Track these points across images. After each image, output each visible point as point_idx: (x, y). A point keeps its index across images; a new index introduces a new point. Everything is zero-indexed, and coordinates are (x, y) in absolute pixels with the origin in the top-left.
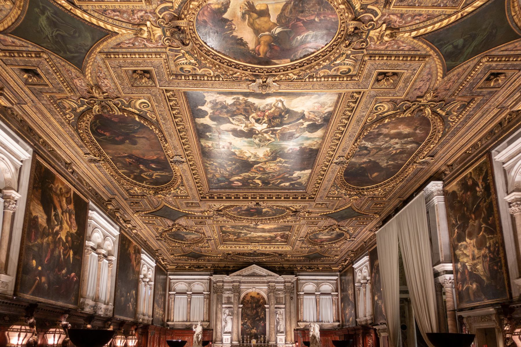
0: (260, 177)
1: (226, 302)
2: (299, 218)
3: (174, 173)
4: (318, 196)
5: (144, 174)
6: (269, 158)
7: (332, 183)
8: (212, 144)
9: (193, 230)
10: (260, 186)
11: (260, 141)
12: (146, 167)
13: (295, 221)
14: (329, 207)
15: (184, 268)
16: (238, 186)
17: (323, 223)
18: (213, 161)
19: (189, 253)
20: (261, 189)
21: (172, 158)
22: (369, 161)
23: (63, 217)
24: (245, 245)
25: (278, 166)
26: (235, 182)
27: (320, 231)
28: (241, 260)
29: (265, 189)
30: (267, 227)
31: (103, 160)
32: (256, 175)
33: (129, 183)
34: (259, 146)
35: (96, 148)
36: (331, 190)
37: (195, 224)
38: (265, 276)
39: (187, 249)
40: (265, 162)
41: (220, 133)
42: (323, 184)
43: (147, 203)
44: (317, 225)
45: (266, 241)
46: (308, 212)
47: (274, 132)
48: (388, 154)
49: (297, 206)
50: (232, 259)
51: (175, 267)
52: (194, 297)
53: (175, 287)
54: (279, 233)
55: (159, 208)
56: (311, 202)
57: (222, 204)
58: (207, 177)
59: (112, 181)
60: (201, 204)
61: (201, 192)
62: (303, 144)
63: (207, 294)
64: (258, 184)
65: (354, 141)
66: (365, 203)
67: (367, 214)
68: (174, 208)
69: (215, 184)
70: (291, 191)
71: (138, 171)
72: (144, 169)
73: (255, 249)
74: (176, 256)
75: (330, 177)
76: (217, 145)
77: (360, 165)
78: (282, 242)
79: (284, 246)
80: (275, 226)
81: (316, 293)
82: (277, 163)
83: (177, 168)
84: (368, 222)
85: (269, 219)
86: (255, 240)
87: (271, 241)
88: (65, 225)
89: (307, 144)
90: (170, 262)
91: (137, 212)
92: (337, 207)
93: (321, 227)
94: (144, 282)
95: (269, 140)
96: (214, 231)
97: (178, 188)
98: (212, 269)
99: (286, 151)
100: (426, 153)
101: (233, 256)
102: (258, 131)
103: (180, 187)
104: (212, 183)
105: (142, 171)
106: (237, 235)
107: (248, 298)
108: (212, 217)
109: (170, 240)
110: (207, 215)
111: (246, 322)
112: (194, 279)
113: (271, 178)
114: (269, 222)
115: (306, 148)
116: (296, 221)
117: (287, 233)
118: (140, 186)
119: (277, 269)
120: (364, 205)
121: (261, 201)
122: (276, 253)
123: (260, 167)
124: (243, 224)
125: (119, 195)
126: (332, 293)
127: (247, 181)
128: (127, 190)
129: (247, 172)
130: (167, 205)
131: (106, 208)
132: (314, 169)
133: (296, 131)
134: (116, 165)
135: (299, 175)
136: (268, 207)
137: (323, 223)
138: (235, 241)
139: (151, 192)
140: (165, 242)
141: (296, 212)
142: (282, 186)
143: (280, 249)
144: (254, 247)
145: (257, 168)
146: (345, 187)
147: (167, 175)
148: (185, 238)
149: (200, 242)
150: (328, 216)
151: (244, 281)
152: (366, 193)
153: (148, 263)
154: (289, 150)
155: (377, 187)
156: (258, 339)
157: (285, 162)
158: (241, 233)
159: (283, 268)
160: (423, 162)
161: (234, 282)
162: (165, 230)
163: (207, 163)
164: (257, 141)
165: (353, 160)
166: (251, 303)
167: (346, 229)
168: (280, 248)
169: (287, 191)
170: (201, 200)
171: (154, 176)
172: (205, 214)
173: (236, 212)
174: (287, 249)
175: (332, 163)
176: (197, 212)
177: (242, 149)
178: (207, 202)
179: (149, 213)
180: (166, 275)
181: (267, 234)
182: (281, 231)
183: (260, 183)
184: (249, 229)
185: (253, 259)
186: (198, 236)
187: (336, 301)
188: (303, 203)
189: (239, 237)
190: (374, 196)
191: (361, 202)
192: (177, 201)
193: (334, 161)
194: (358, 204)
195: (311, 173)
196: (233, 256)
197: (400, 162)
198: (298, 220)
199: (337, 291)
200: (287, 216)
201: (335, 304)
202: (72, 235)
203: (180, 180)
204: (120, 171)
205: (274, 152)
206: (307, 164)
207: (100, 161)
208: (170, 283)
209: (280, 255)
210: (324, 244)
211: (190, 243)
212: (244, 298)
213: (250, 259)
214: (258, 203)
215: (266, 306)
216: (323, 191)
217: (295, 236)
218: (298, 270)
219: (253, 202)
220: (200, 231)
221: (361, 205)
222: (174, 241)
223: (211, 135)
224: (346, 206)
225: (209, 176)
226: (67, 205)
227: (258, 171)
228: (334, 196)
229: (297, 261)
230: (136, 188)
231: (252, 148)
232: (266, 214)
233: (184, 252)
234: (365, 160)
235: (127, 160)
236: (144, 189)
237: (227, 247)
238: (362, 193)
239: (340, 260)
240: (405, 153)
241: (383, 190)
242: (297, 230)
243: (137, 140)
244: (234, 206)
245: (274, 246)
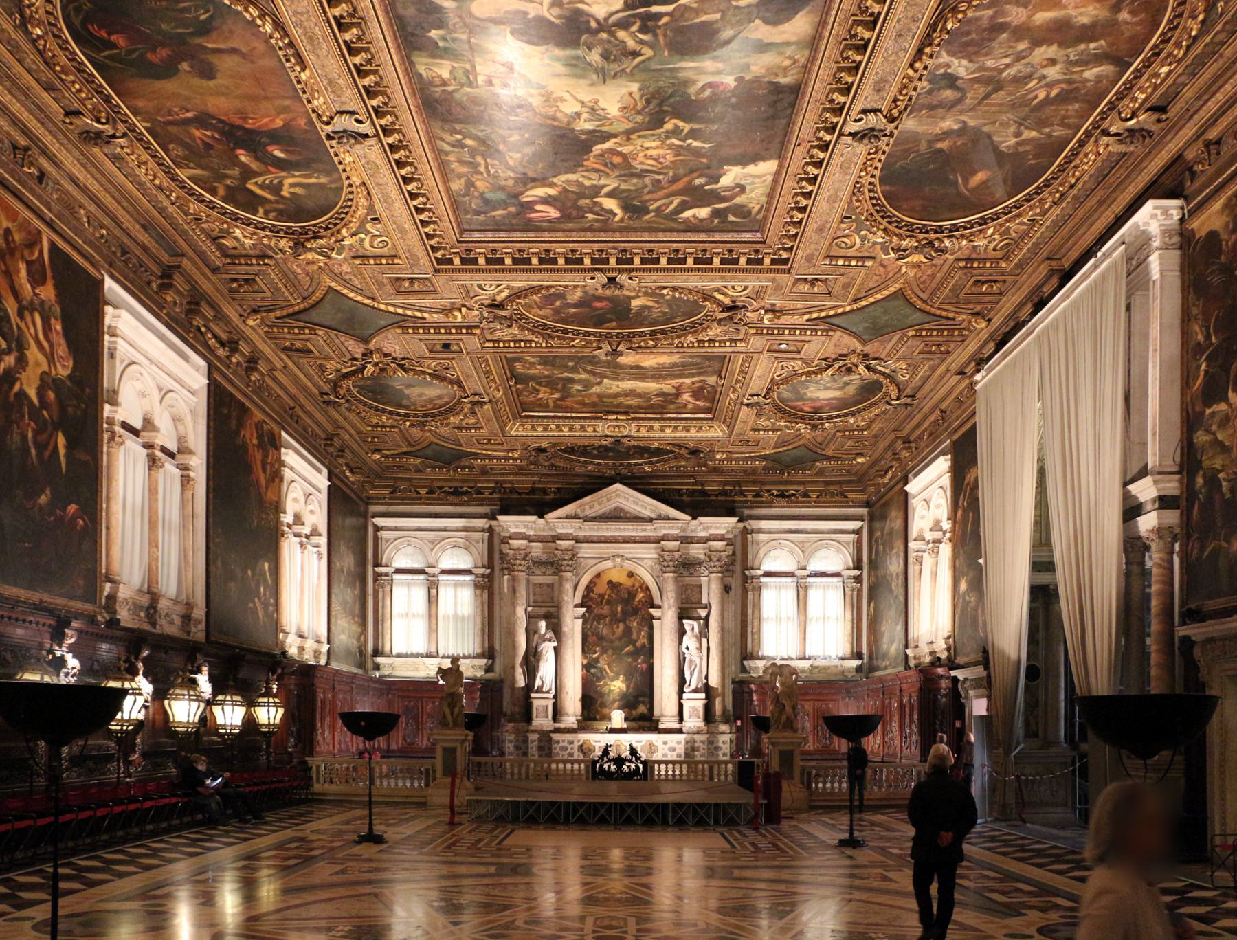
0: (615, 190)
2: (743, 329)
3: (344, 175)
4: (800, 254)
5: (256, 183)
6: (639, 118)
7: (841, 206)
8: (451, 72)
9: (425, 373)
10: (617, 218)
11: (606, 56)
12: (257, 159)
13: (731, 341)
14: (834, 293)
15: (415, 495)
16: (550, 221)
17: (818, 347)
18: (460, 133)
19: (423, 445)
20: (621, 230)
21: (328, 123)
22: (960, 130)
23: (23, 325)
24: (587, 422)
25: (671, 147)
26: (538, 207)
27: (808, 374)
28: (578, 469)
29: (636, 230)
30: (650, 361)
31: (124, 135)
32: (602, 182)
33: (214, 213)
34: (604, 76)
35: (97, 92)
36: (839, 233)
37: (431, 352)
39: (416, 433)
40: (628, 134)
41: (471, 32)
42: (813, 212)
43: (276, 281)
44: (799, 352)
45: (651, 406)
46: (772, 310)
47: (650, 24)
48: (1024, 102)
49: (736, 287)
50: (552, 465)
54: (688, 381)
55: (314, 298)
56: (778, 276)
57: (505, 284)
58: (448, 190)
59: (165, 209)
60: (440, 281)
61: (433, 242)
62: (747, 67)
64: (611, 212)
65: (911, 51)
66: (944, 279)
67: (951, 315)
68: (359, 298)
69: (478, 213)
70: (717, 237)
71: (236, 172)
72: (254, 166)
73: (617, 433)
74: (387, 457)
75: (837, 185)
76: (467, 73)
77: (930, 143)
78: (697, 410)
79: (705, 425)
80: (675, 358)
82: (667, 138)
83: (348, 159)
84: (952, 345)
85: (653, 333)
86: (618, 406)
87: (662, 407)
88: (33, 353)
89: (760, 65)
91: (255, 311)
92: (858, 290)
93: (812, 360)
94: (297, 535)
95: (635, 54)
96: (488, 374)
97: (361, 228)
98: (496, 496)
99: (692, 91)
100: (1143, 96)
101: (553, 456)
102: (598, 21)
103: (368, 226)
104: (467, 212)
105: (248, 174)
106: (560, 386)
108: (477, 327)
109: (365, 404)
110: (459, 319)
113: (650, 192)
114: (651, 343)
115: (756, 80)
116: (736, 341)
117: (712, 380)
118: (249, 225)
119: (685, 498)
120: (941, 283)
121: (624, 270)
122: (680, 446)
123: (612, 151)
124: (573, 350)
125: (191, 253)
127: (576, 201)
128: (215, 239)
129: (572, 170)
130: (339, 288)
131: (161, 300)
132: (785, 158)
133: (722, 18)
134: (166, 150)
135: (738, 181)
136: (646, 294)
137: (818, 347)
138: (557, 408)
139: (284, 244)
140: (349, 410)
141: (733, 308)
142: (687, 221)
143: (693, 433)
144: (615, 427)
145: (602, 155)
146: (884, 222)
147: (322, 186)
148: (408, 397)
149: (451, 410)
150: (829, 324)
152: (947, 243)
153: (305, 480)
154: (703, 89)
155: (983, 221)
157: (693, 134)
158: (572, 381)
159: (704, 493)
160: (1131, 131)
162: (345, 371)
163: (443, 140)
164: (595, 57)
165: (909, 124)
167: (886, 367)
168: (693, 430)
169: (702, 237)
170: (436, 271)
171: (286, 187)
172: (455, 317)
173: (547, 312)
174: (711, 434)
175: (841, 134)
176: (429, 312)
177: (550, 88)
178: (455, 276)
179: (288, 316)
181: (651, 386)
182: (693, 375)
183: (618, 211)
184: (596, 369)
185: (615, 467)
186: (445, 392)
188: (754, 276)
189: (566, 393)
190: (974, 256)
191: (933, 276)
192: (367, 272)
193: (847, 130)
194: (924, 282)
195: (777, 174)
196: (553, 456)
197: (1058, 132)
198: (740, 337)
200: (706, 324)
202: (57, 384)
203: (363, 202)
204: (182, 174)
205: (653, 97)
206: (762, 141)
207: (114, 136)
209: (695, 452)
211: (425, 416)
213: (607, 466)
214: (615, 279)
216: (815, 237)
217: (735, 390)
218: (747, 502)
219: (598, 275)
220: (447, 373)
221: (934, 285)
222: (376, 409)
223: (444, 39)
224: (886, 288)
225: (456, 186)
226: (33, 288)
227: (606, 165)
228: (850, 253)
229: (745, 472)
230: (237, 231)
231: (582, 82)
232: (640, 318)
233: (410, 444)
234: (949, 124)
235: (197, 133)
236: (262, 233)
237: (533, 426)
238: (936, 243)
239: (872, 471)
240: (1076, 100)
241: (1001, 235)
242: (741, 371)
243: (214, 59)
244: (540, 288)
245: (673, 424)
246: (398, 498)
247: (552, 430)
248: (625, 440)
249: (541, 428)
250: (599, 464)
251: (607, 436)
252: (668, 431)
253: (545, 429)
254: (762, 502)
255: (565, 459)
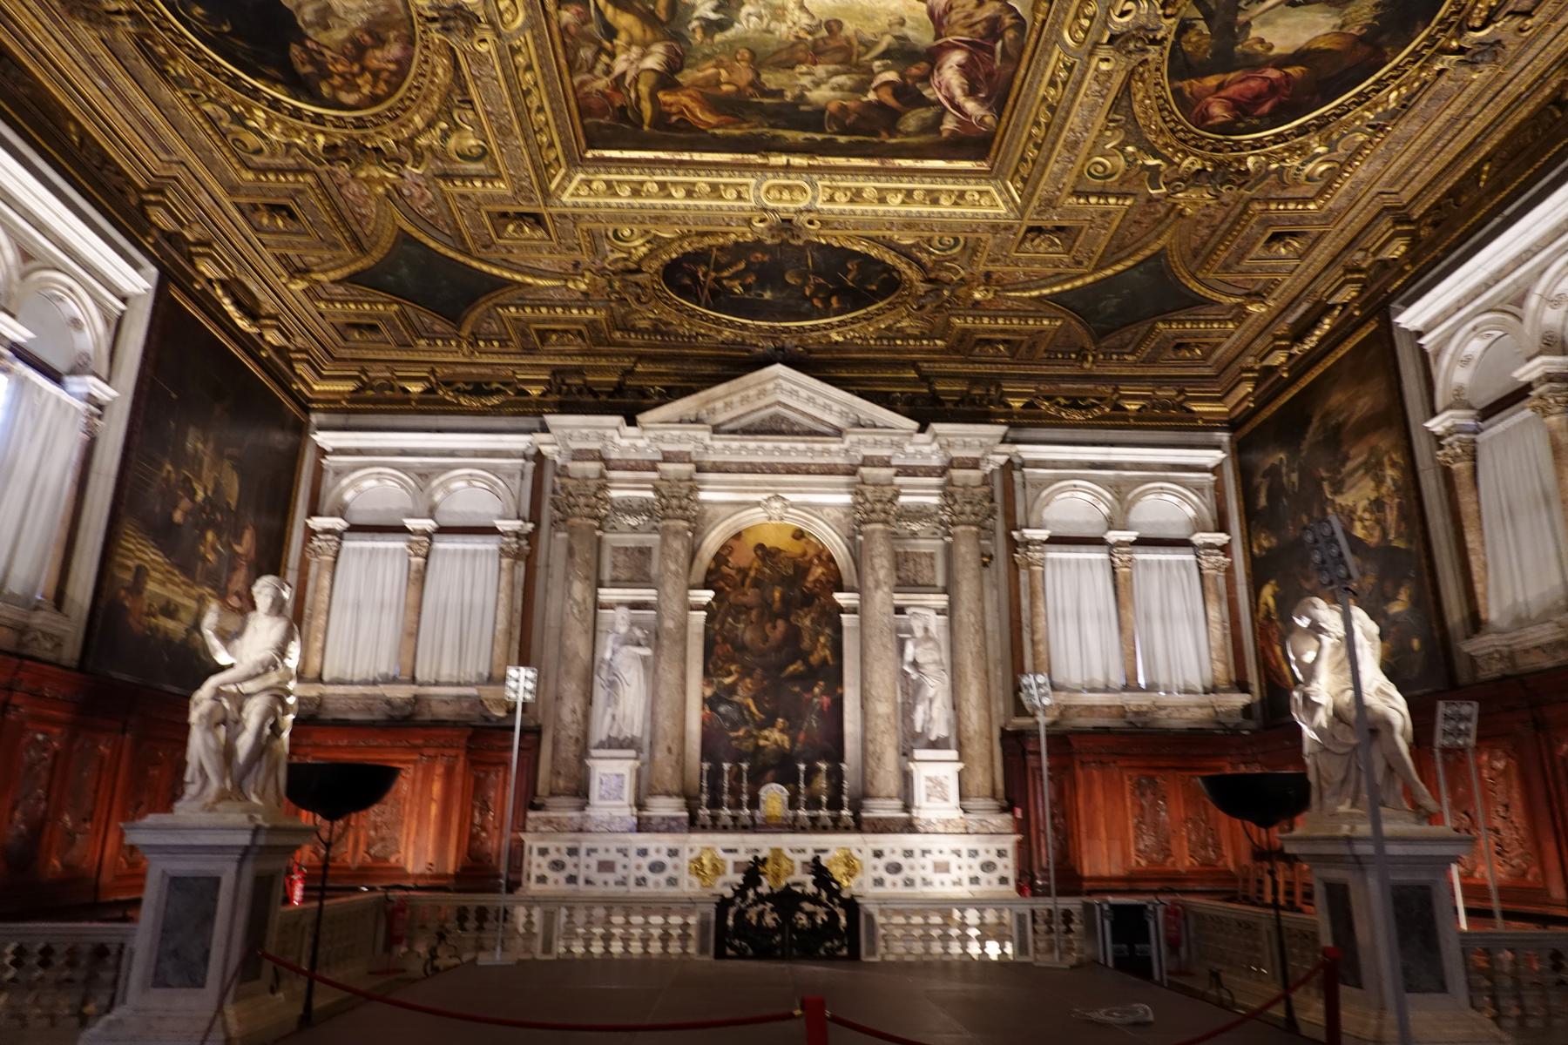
1: (624, 574)
15: (400, 395)
38: (839, 433)
51: (348, 387)
52: (443, 544)
53: (341, 494)
63: (517, 535)
73: (787, 205)
79: (971, 187)
81: (1113, 536)
90: (317, 352)
98: (550, 398)
107: (744, 557)
111: (731, 690)
112: (452, 453)
126: (1199, 538)
143: (946, 207)
151: (719, 458)
156: (796, 782)
161: (668, 458)
166: (757, 583)
168: (944, 200)
180: (301, 430)
187: (1222, 582)
199: (1222, 526)
201: (1219, 598)
208: (319, 471)
210: (1238, 146)
212: (720, 557)
215: (842, 598)
246: (368, 401)
247: (649, 195)
248: (805, 217)
249: (626, 191)
250: (744, 327)
251: (765, 210)
252: (895, 202)
253: (636, 193)
254: (1040, 416)
255: (680, 309)
